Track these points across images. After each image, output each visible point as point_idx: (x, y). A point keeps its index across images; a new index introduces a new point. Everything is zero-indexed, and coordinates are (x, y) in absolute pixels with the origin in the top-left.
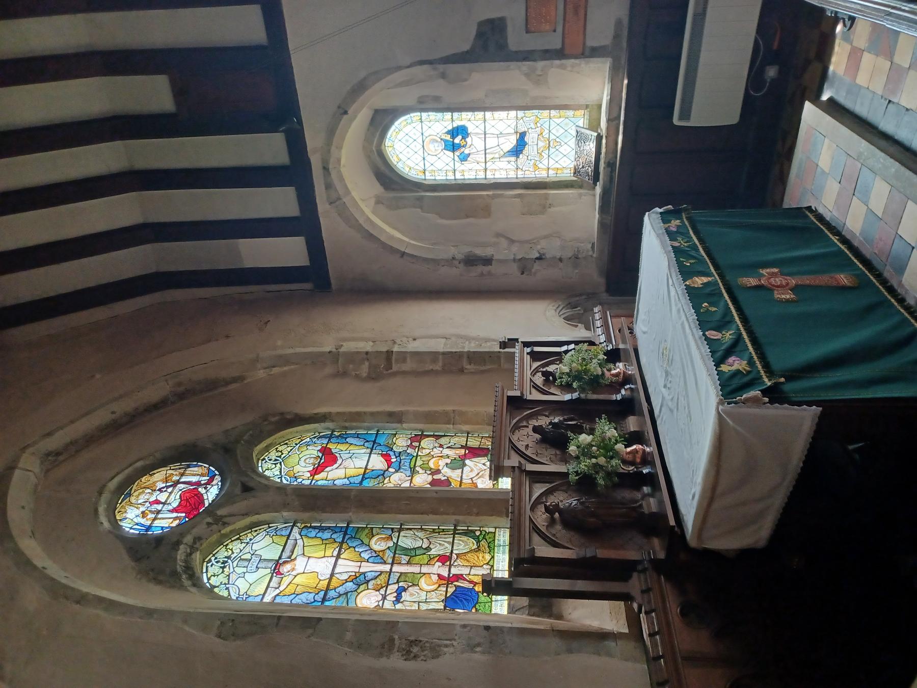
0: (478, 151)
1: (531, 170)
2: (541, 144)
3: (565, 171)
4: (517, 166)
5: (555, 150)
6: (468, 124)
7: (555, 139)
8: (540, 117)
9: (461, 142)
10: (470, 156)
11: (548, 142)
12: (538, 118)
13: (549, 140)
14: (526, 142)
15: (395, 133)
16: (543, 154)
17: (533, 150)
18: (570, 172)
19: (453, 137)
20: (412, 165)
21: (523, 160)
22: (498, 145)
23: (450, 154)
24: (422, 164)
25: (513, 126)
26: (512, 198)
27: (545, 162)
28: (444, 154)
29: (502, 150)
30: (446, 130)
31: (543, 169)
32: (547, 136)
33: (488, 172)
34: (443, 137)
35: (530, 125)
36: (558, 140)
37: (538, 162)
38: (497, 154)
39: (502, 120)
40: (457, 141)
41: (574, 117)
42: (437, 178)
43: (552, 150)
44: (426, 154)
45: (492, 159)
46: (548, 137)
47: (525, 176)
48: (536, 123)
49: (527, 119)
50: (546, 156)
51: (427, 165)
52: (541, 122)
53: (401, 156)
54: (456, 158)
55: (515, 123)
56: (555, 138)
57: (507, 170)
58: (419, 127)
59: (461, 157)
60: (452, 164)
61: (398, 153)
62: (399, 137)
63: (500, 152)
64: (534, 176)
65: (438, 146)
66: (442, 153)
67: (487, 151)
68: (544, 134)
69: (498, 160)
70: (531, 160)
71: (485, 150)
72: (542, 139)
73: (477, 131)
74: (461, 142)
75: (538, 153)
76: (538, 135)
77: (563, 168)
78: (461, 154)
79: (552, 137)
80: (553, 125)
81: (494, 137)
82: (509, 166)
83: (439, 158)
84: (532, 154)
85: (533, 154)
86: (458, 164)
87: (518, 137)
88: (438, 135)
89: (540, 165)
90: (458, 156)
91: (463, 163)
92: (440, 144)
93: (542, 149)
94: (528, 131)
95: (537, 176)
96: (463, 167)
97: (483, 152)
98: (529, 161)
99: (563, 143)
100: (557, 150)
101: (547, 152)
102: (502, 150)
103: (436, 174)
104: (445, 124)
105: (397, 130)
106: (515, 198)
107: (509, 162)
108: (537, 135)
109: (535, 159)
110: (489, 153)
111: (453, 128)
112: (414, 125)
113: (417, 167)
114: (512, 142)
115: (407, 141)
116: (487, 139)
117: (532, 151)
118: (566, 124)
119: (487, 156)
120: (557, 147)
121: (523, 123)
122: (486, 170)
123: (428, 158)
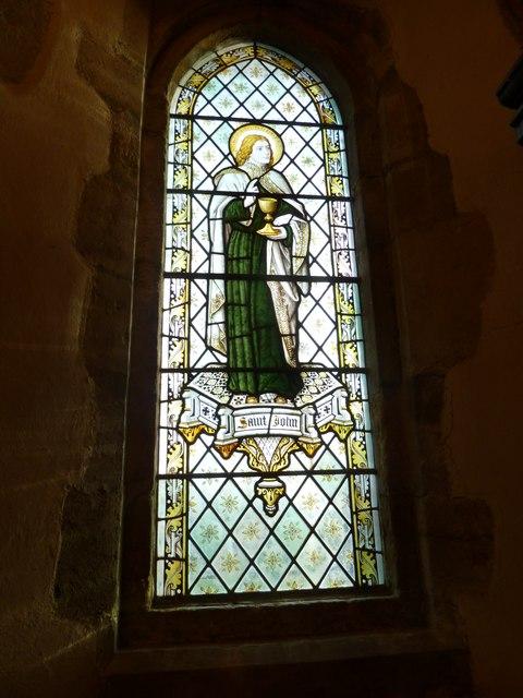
1: (183, 419)
2: (268, 447)
4: (199, 371)
5: (250, 495)
7: (284, 494)
12: (348, 435)
13: (281, 472)
16: (237, 456)
17: (250, 422)
24: (209, 111)
25: (320, 358)
31: (186, 457)
32: (295, 466)
33: (179, 284)
35: (327, 410)
36: (283, 502)
37: (209, 440)
39: (336, 328)
41: (355, 549)
43: (248, 485)
44: (235, 125)
48: (330, 430)
49: (343, 403)
50: (229, 465)
51: (210, 126)
52: (336, 446)
53: (233, 71)
55: (330, 366)
56: (290, 494)
58: (305, 118)
61: (241, 66)
62: (279, 73)
68: (300, 455)
70: (217, 416)
72: (283, 451)
75: (241, 439)
76: (296, 438)
80: (330, 484)
84: (238, 419)
85: (238, 423)
88: (286, 161)
89: (198, 449)
93: (252, 450)
98: (211, 414)
100: (250, 504)
101: (244, 467)
108: (299, 434)
109: (222, 431)
112: (312, 109)
113: (201, 101)
117: (247, 418)
122: (190, 276)
123: (226, 130)
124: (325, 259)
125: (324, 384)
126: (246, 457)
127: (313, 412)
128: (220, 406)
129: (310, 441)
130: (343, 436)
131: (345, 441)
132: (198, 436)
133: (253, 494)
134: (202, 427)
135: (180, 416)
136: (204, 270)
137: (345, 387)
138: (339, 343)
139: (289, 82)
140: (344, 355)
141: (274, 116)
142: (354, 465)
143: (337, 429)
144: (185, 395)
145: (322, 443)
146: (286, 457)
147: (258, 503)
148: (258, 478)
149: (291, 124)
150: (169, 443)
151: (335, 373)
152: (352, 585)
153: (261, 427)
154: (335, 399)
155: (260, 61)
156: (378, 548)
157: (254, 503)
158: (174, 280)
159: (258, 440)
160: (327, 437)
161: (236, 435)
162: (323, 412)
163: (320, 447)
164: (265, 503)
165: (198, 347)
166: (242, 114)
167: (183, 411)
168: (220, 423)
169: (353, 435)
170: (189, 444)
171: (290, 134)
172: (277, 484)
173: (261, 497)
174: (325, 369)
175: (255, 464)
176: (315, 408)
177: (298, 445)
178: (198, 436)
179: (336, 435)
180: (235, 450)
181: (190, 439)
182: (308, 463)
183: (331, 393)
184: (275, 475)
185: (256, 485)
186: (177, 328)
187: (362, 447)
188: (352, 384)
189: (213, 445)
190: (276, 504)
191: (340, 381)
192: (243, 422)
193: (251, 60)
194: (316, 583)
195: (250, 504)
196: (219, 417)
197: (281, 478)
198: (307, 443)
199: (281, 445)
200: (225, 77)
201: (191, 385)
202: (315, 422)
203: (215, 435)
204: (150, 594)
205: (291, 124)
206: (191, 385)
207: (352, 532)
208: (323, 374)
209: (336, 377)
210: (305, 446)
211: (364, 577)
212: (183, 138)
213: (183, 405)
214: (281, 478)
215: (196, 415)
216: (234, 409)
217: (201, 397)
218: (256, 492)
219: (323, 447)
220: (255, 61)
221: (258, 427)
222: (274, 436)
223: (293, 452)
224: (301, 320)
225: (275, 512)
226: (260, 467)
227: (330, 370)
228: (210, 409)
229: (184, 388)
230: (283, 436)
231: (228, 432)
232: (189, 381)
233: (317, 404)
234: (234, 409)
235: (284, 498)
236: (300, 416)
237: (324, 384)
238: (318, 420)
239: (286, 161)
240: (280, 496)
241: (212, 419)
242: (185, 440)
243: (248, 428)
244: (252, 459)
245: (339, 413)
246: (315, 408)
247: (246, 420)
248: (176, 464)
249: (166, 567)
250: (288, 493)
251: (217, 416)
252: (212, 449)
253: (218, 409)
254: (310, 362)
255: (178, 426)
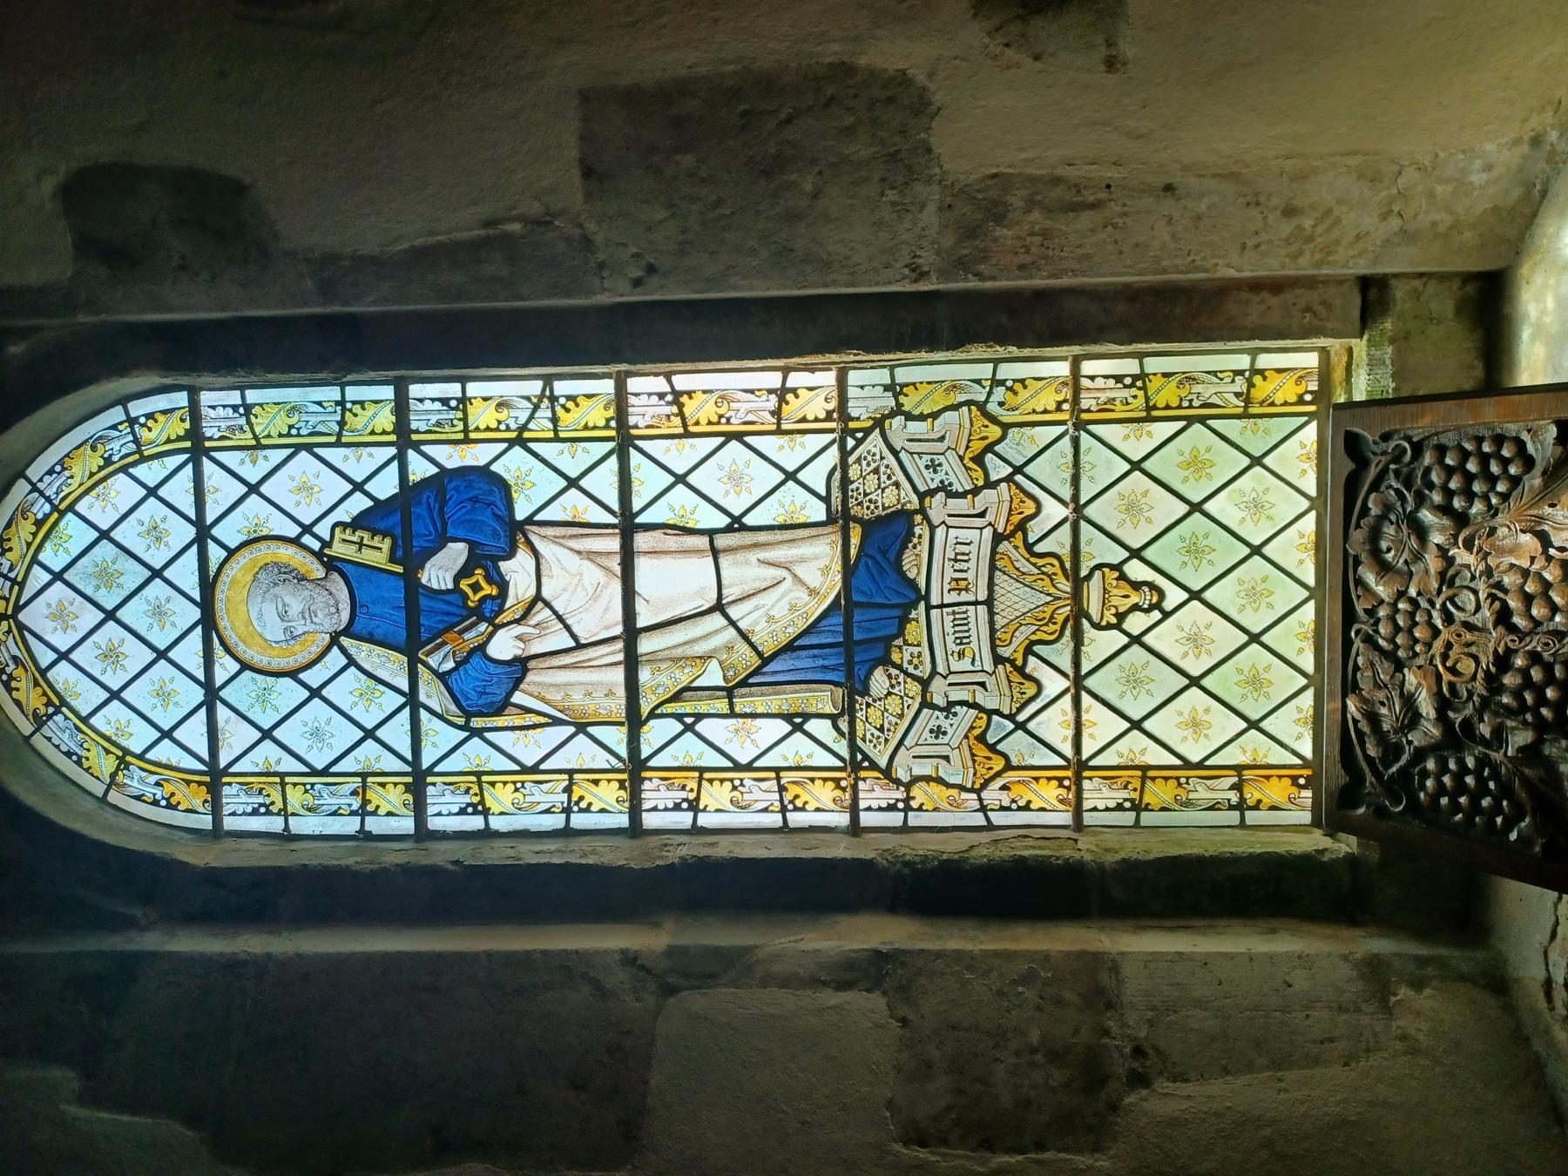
0: (580, 646)
2: (1016, 599)
3: (1202, 792)
4: (853, 748)
5: (1116, 639)
6: (512, 465)
8: (1008, 418)
9: (464, 584)
10: (530, 677)
11: (1065, 586)
12: (994, 420)
14: (912, 584)
15: (25, 529)
17: (960, 641)
18: (1234, 797)
19: (411, 557)
20: (138, 737)
21: (893, 704)
22: (719, 607)
23: (392, 667)
24: (194, 734)
25: (816, 476)
26: (815, 983)
27: (1054, 725)
28: (352, 662)
29: (744, 636)
30: (359, 503)
32: (1059, 543)
34: (338, 549)
35: (934, 467)
36: (1136, 570)
38: (714, 664)
40: (439, 572)
41: (1245, 415)
42: (299, 826)
43: (1100, 643)
44: (225, 667)
45: (676, 697)
46: (1065, 552)
47: (915, 820)
48: (979, 459)
49: (916, 428)
50: (1054, 684)
52: (1017, 447)
53: (63, 675)
54: (432, 694)
55: (833, 455)
56: (1117, 555)
57: (787, 777)
58: (180, 491)
59: (467, 683)
60: (397, 733)
61: (45, 657)
62: (53, 557)
63: (729, 648)
64: (979, 820)
65: (308, 614)
66: (335, 659)
67: (646, 645)
68: (1035, 530)
69: (722, 706)
71: (631, 633)
72: (1026, 567)
73: (574, 505)
74: (464, 584)
75: (998, 660)
76: (998, 538)
77: (1187, 765)
78: (459, 664)
79: (1097, 550)
80: (1101, 467)
81: (697, 552)
82: (799, 749)
83: (315, 693)
84: (956, 666)
85: (965, 664)
86: (439, 737)
87: (853, 552)
88: (307, 540)
89: (1018, 746)
90: (442, 677)
91: (477, 723)
92: (321, 598)
93: (1022, 635)
94: (922, 511)
95: (998, 818)
96: (476, 754)
97: (616, 652)
98: (939, 719)
99: (1174, 596)
100: (1136, 640)
102: (744, 636)
103: (295, 797)
104: (358, 464)
105: (42, 508)
106: (842, 986)
107: (797, 721)
108: (988, 533)
109: (980, 699)
110: (654, 658)
111: (409, 491)
112: (150, 473)
113: (166, 752)
114: (813, 579)
115: (106, 576)
116: (642, 566)
117: (952, 647)
118: (1196, 464)
119: (644, 675)
120: (1136, 623)
121: (891, 460)
122: (635, 769)
124: (572, 460)
125: (876, 471)
126: (1036, 648)
127: (940, 496)
128: (926, 704)
129: (1006, 506)
130: (995, 432)
131: (1006, 427)
132: (992, 748)
133: (1115, 632)
134: (972, 741)
135: (949, 786)
136: (616, 738)
137: (879, 423)
138: (779, 432)
139: (74, 533)
140: (804, 420)
141: (186, 573)
142: (1059, 409)
143: (977, 446)
144: (903, 775)
145: (1009, 479)
146: (1040, 562)
147: (1136, 623)
148: (1085, 622)
149: (203, 534)
150: (1008, 809)
151: (851, 443)
152: (1314, 425)
153: (972, 620)
154: (908, 445)
155: (18, 608)
156: (1243, 362)
157: (1136, 632)
158: (646, 805)
159: (999, 621)
160: (999, 470)
161: (989, 667)
162: (940, 476)
163: (1018, 486)
164: (1136, 607)
165: (799, 749)
166: (190, 653)
167: (940, 781)
168: (962, 703)
169: (992, 407)
170: (1009, 767)
171: (229, 531)
172: (1095, 584)
173: (1121, 617)
174: (844, 464)
175: (1052, 628)
176: (932, 493)
177: (1012, 534)
178: (992, 748)
179: (989, 448)
180: (1021, 670)
181: (998, 764)
182: (1054, 511)
183: (895, 453)
184: (1078, 583)
185: (1097, 627)
186: (757, 795)
187: (1018, 386)
188: (873, 405)
189: (1011, 717)
190: (1137, 586)
191: (867, 432)
192: (961, 655)
193: (22, 627)
194: (1305, 504)
195: (1136, 640)
196: (951, 704)
197: (1084, 573)
198: (1010, 514)
199: (1014, 573)
200: (85, 697)
201: (883, 762)
202: (963, 495)
203: (990, 713)
204: (1317, 841)
205: (203, 534)
206: (883, 763)
207: (1202, 420)
208: (853, 472)
209: (859, 442)
210: (1016, 519)
211: (1301, 401)
212: (276, 796)
213: (927, 779)
214: (1084, 573)
215: (945, 751)
216: (934, 672)
217: (907, 742)
218: (1109, 627)
219: (1019, 478)
220: (22, 617)
221: (972, 625)
222: (991, 584)
223: (1029, 547)
224: (723, 521)
225: (1152, 586)
226: (1060, 619)
227: (844, 454)
228: (933, 724)
229: (887, 773)
230: (993, 567)
231: (982, 685)
232: (874, 766)
233: (922, 488)
234: (934, 672)
235: (1127, 568)
236: (948, 527)
237: (876, 471)
238: (957, 487)
239: (307, 540)
240: (1123, 577)
241: (955, 721)
242: (998, 774)
243: (974, 645)
244: (1040, 636)
245: (942, 439)
246: (932, 493)
247: (957, 649)
248: (1050, 793)
249: (1256, 807)
250: (1115, 561)
251: (949, 708)
252: (1021, 718)
253: (934, 707)
254: (826, 500)
255: (971, 790)
